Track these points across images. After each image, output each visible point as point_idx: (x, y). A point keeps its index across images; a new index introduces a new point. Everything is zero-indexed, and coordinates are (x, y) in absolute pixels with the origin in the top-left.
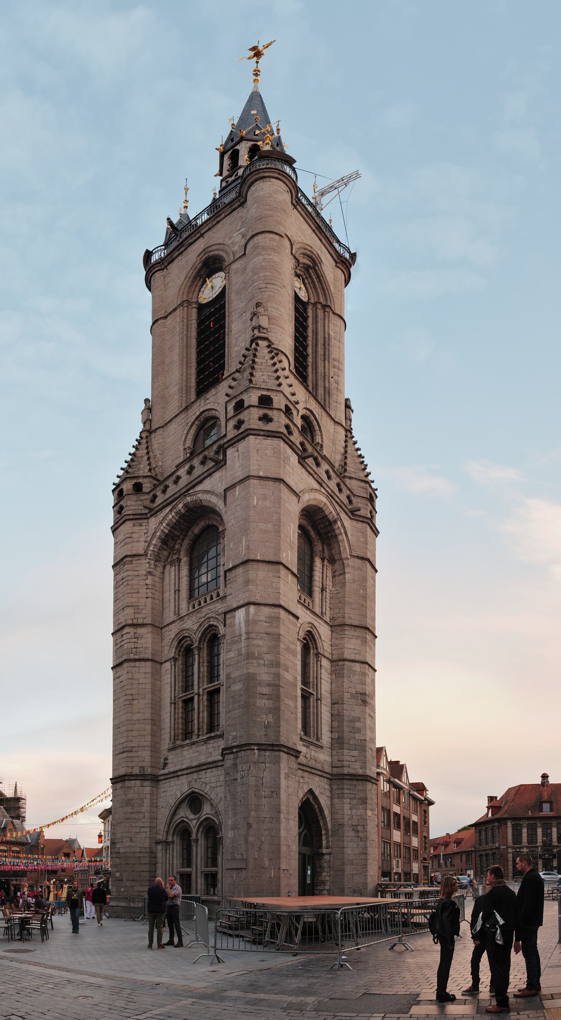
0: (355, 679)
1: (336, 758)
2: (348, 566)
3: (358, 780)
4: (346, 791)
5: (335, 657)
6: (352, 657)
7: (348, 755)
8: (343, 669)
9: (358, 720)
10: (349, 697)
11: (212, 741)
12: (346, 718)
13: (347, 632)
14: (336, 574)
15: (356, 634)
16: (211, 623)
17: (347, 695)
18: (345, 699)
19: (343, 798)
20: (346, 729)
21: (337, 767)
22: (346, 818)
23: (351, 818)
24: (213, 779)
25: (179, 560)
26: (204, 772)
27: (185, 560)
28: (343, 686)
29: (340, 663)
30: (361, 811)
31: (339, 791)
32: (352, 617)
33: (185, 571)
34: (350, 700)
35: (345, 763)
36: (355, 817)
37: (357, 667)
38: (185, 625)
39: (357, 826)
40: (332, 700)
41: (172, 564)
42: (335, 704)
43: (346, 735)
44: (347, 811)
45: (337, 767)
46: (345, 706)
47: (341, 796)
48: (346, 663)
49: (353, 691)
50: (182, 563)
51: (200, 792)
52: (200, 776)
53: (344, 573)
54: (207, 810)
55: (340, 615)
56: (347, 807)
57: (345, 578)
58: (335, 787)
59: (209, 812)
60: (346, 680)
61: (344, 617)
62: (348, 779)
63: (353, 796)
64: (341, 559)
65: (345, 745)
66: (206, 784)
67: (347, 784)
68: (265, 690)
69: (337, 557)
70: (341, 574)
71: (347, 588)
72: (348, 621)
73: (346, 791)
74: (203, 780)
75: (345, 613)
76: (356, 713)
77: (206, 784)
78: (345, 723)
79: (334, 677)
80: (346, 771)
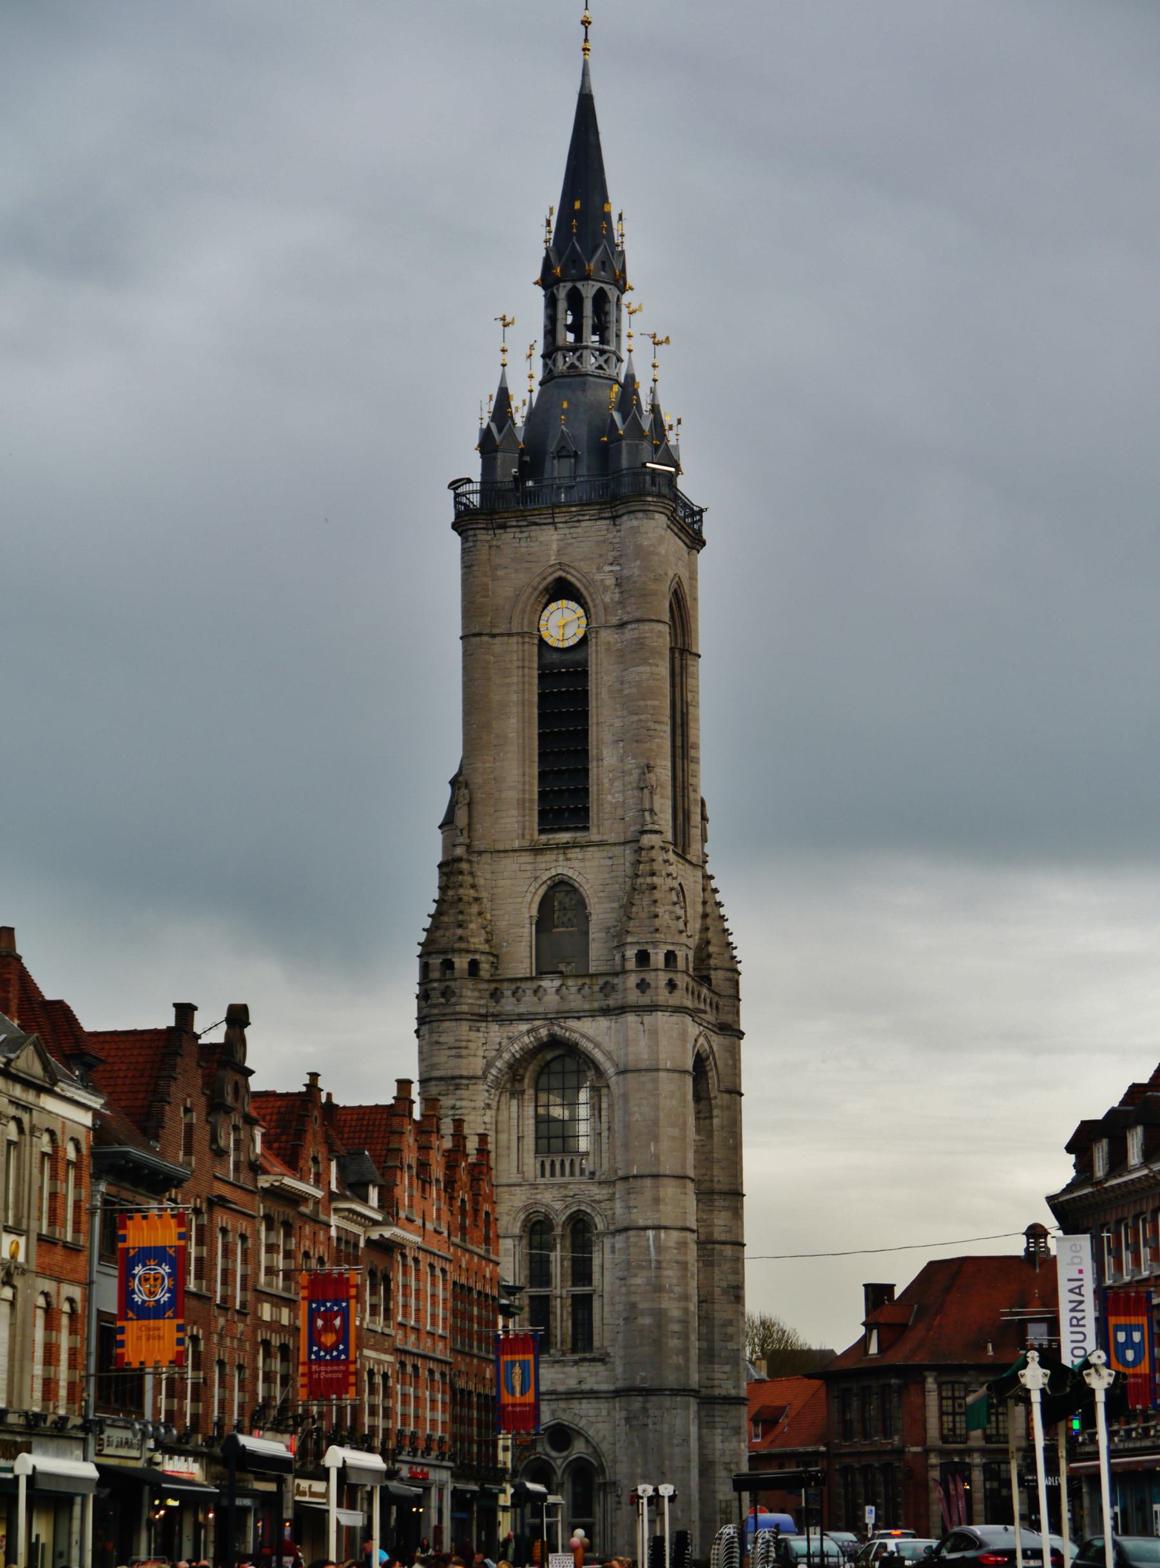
0: (726, 1267)
1: (704, 1375)
2: (716, 1107)
3: (730, 1404)
4: (717, 1419)
5: (702, 1238)
6: (723, 1237)
7: (720, 1371)
8: (712, 1255)
9: (730, 1323)
10: (720, 1293)
11: (586, 1364)
12: (716, 1322)
13: (716, 1204)
14: (701, 1115)
15: (726, 1204)
16: (583, 1208)
17: (717, 1291)
18: (716, 1297)
19: (714, 1428)
20: (717, 1337)
21: (706, 1387)
22: (718, 1453)
23: (723, 1455)
24: (591, 1413)
25: (523, 1092)
26: (576, 1402)
27: (530, 1092)
28: (713, 1279)
29: (709, 1246)
30: (734, 1445)
31: (709, 1419)
32: (719, 1177)
33: (530, 1111)
34: (721, 1297)
35: (716, 1383)
36: (727, 1452)
37: (728, 1251)
38: (539, 1197)
39: (730, 1463)
40: (699, 1296)
41: (513, 1095)
42: (703, 1302)
43: (718, 1345)
44: (719, 1446)
45: (706, 1387)
46: (716, 1307)
47: (711, 1425)
48: (717, 1246)
49: (724, 1284)
50: (526, 1097)
51: (571, 1425)
52: (572, 1406)
53: (711, 1117)
54: (579, 1448)
55: (707, 1178)
56: (718, 1439)
57: (712, 1124)
58: (703, 1413)
59: (583, 1450)
60: (716, 1270)
61: (712, 1181)
62: (719, 1403)
63: (725, 1425)
64: (709, 1099)
65: (716, 1359)
66: (581, 1417)
67: (718, 1410)
68: (676, 1327)
69: (703, 1094)
70: (706, 1118)
71: (716, 1139)
72: (717, 1187)
73: (717, 1419)
74: (577, 1411)
75: (713, 1176)
76: (728, 1315)
77: (581, 1417)
78: (716, 1330)
79: (701, 1264)
80: (717, 1392)
